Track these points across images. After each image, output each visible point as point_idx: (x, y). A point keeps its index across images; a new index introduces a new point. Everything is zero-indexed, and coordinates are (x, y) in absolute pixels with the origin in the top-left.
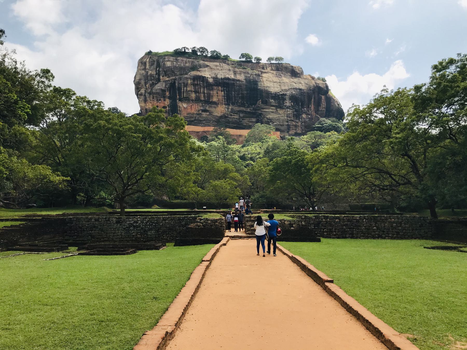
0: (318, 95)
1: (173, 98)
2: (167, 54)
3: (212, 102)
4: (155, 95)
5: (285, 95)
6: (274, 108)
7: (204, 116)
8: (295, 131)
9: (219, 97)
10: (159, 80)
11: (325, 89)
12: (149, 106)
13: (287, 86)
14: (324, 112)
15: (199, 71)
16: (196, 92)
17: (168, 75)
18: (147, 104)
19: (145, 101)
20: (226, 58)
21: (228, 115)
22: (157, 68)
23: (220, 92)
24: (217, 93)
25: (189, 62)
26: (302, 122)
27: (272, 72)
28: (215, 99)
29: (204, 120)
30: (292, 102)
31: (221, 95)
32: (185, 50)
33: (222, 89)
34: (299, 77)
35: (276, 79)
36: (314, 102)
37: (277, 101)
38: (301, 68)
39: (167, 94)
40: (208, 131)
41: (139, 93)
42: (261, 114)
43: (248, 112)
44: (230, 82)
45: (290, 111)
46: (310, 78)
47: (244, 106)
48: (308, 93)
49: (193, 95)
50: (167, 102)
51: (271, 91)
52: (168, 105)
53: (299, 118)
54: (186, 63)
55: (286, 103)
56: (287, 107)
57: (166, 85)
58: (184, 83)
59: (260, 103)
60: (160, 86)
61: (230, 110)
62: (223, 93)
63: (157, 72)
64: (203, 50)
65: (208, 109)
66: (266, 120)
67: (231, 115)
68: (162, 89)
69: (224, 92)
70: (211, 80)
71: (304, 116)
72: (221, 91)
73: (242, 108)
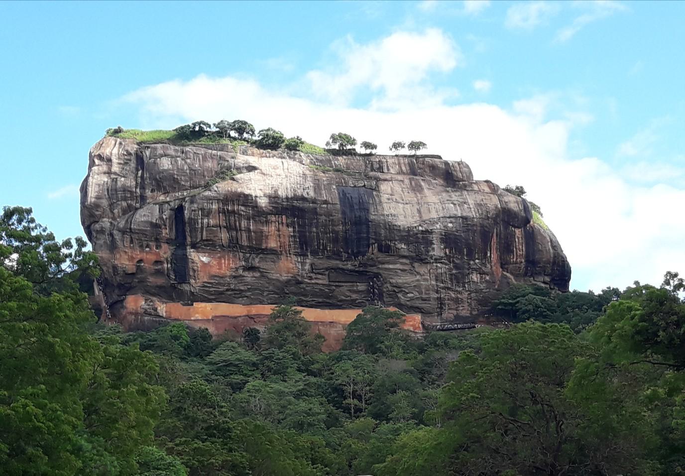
0: (506, 228)
2: (156, 136)
3: (266, 249)
4: (135, 236)
5: (430, 232)
6: (407, 261)
7: (249, 279)
8: (455, 312)
9: (282, 240)
11: (523, 214)
12: (125, 261)
13: (433, 211)
14: (523, 265)
16: (229, 228)
17: (165, 188)
18: (118, 256)
19: (113, 247)
20: (293, 147)
21: (303, 277)
22: (137, 170)
23: (285, 228)
24: (279, 231)
25: (212, 157)
26: (471, 292)
27: (400, 177)
28: (272, 244)
31: (287, 233)
32: (200, 127)
33: (289, 221)
34: (464, 188)
35: (410, 197)
36: (499, 243)
37: (412, 248)
38: (467, 166)
40: (259, 316)
41: (97, 226)
42: (377, 275)
44: (306, 205)
45: (442, 268)
46: (487, 189)
48: (482, 226)
49: (224, 236)
50: (166, 252)
51: (399, 223)
53: (464, 283)
54: (205, 158)
55: (433, 249)
56: (436, 259)
57: (161, 211)
58: (202, 209)
59: (376, 251)
60: (146, 215)
61: (307, 267)
62: (291, 229)
63: (139, 180)
64: (241, 128)
65: (258, 264)
66: (390, 288)
68: (151, 223)
69: (294, 228)
70: (263, 202)
71: (475, 277)
72: (288, 226)
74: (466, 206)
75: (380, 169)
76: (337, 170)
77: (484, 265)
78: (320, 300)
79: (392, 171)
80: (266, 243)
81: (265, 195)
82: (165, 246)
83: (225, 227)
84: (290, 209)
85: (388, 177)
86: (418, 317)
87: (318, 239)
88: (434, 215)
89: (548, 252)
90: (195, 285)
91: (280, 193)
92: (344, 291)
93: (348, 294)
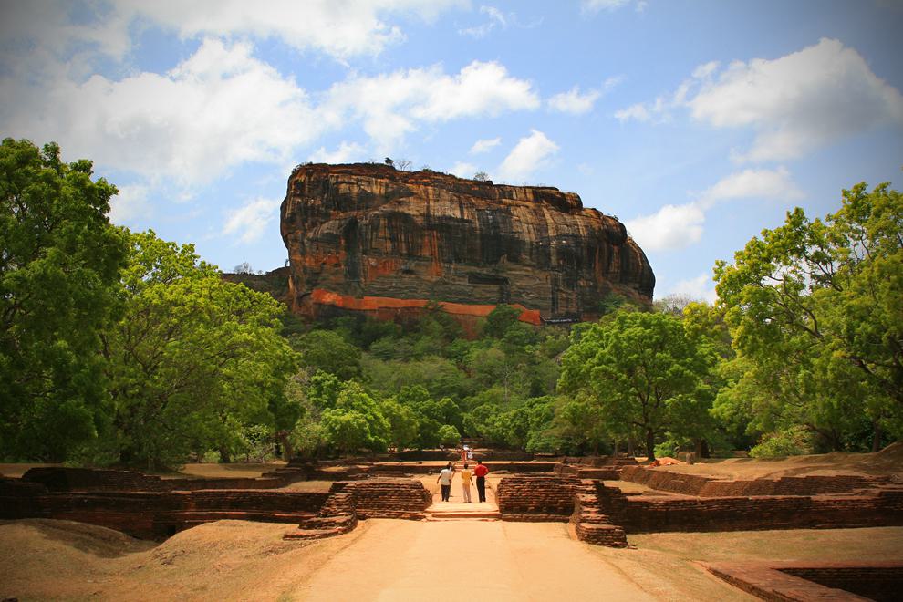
3: (421, 256)
4: (320, 244)
6: (529, 269)
10: (327, 217)
16: (393, 239)
18: (307, 259)
19: (303, 254)
21: (448, 278)
27: (527, 204)
28: (426, 253)
29: (406, 288)
38: (579, 197)
39: (343, 241)
42: (505, 281)
44: (452, 223)
61: (452, 271)
67: (454, 280)
70: (420, 220)
72: (438, 239)
73: (473, 269)
81: (421, 215)
86: (536, 312)
91: (432, 213)
93: (483, 293)
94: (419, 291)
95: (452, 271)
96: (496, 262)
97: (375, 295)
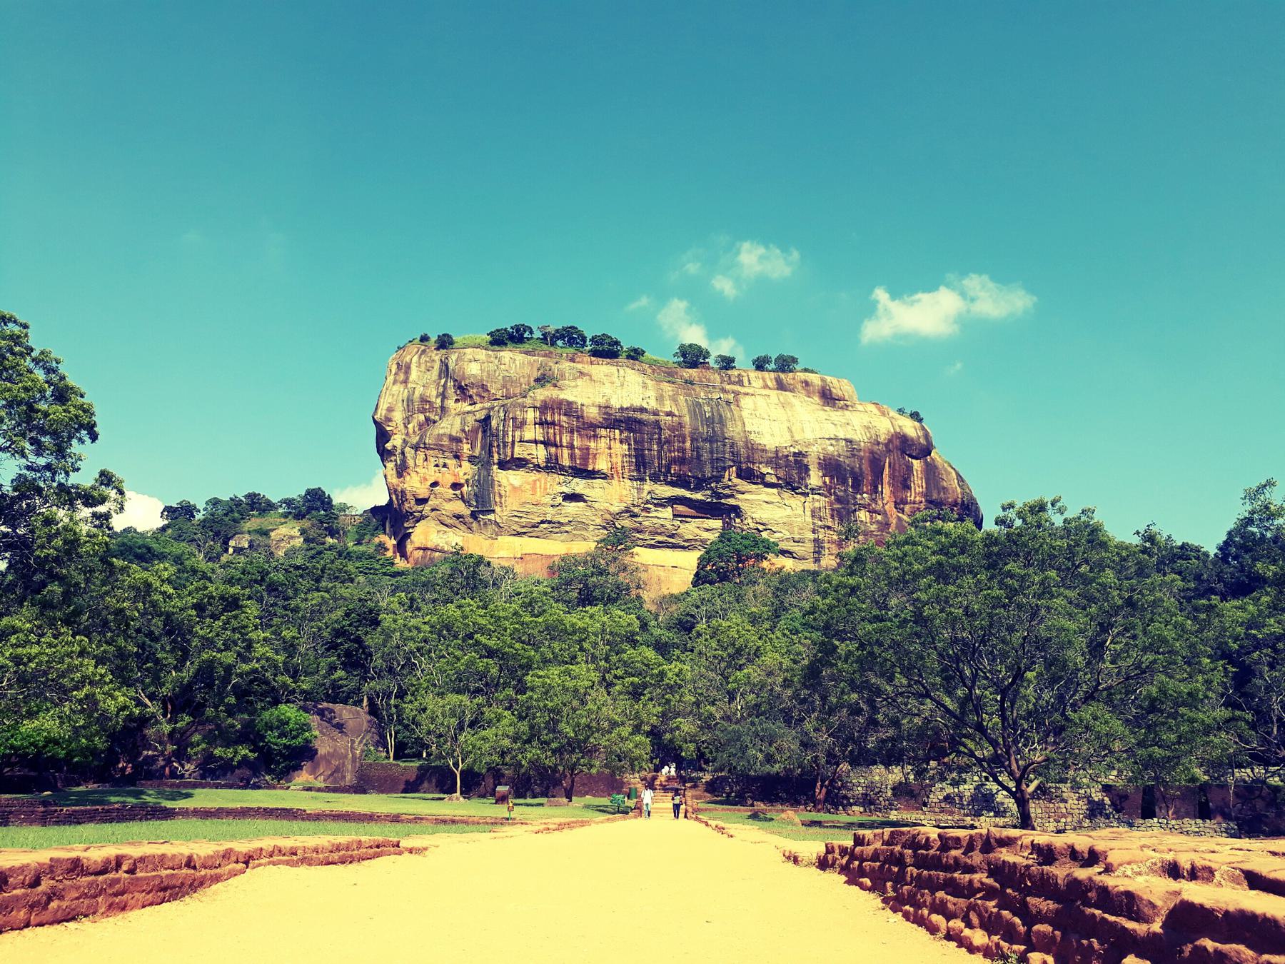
1: (482, 462)
5: (804, 455)
6: (775, 491)
9: (614, 460)
11: (922, 441)
15: (561, 389)
16: (546, 443)
17: (471, 397)
19: (402, 470)
22: (440, 378)
28: (602, 465)
30: (824, 476)
33: (623, 436)
36: (892, 476)
39: (466, 447)
42: (736, 510)
43: (697, 501)
44: (644, 417)
45: (821, 501)
47: (685, 485)
48: (872, 452)
49: (540, 453)
50: (466, 471)
52: (467, 481)
56: (812, 489)
57: (464, 423)
58: (514, 419)
62: (625, 447)
70: (592, 413)
71: (863, 515)
72: (621, 442)
74: (849, 428)
75: (740, 383)
76: (686, 382)
77: (875, 500)
78: (660, 538)
79: (754, 384)
80: (594, 463)
82: (466, 464)
83: (542, 442)
84: (627, 422)
85: (750, 391)
87: (660, 458)
88: (809, 436)
89: (954, 491)
90: (501, 514)
92: (691, 528)
94: (592, 528)
95: (644, 495)
96: (718, 479)
97: (519, 534)
